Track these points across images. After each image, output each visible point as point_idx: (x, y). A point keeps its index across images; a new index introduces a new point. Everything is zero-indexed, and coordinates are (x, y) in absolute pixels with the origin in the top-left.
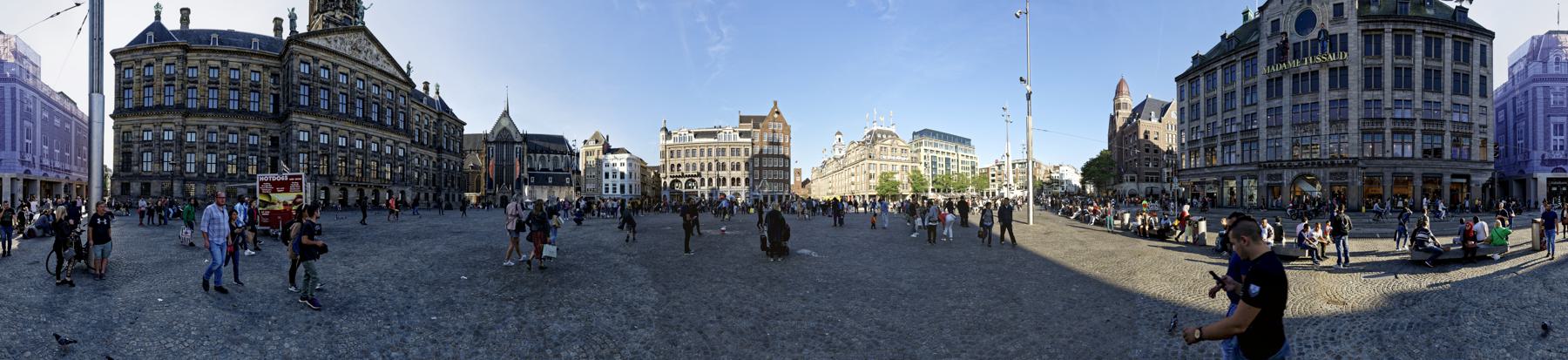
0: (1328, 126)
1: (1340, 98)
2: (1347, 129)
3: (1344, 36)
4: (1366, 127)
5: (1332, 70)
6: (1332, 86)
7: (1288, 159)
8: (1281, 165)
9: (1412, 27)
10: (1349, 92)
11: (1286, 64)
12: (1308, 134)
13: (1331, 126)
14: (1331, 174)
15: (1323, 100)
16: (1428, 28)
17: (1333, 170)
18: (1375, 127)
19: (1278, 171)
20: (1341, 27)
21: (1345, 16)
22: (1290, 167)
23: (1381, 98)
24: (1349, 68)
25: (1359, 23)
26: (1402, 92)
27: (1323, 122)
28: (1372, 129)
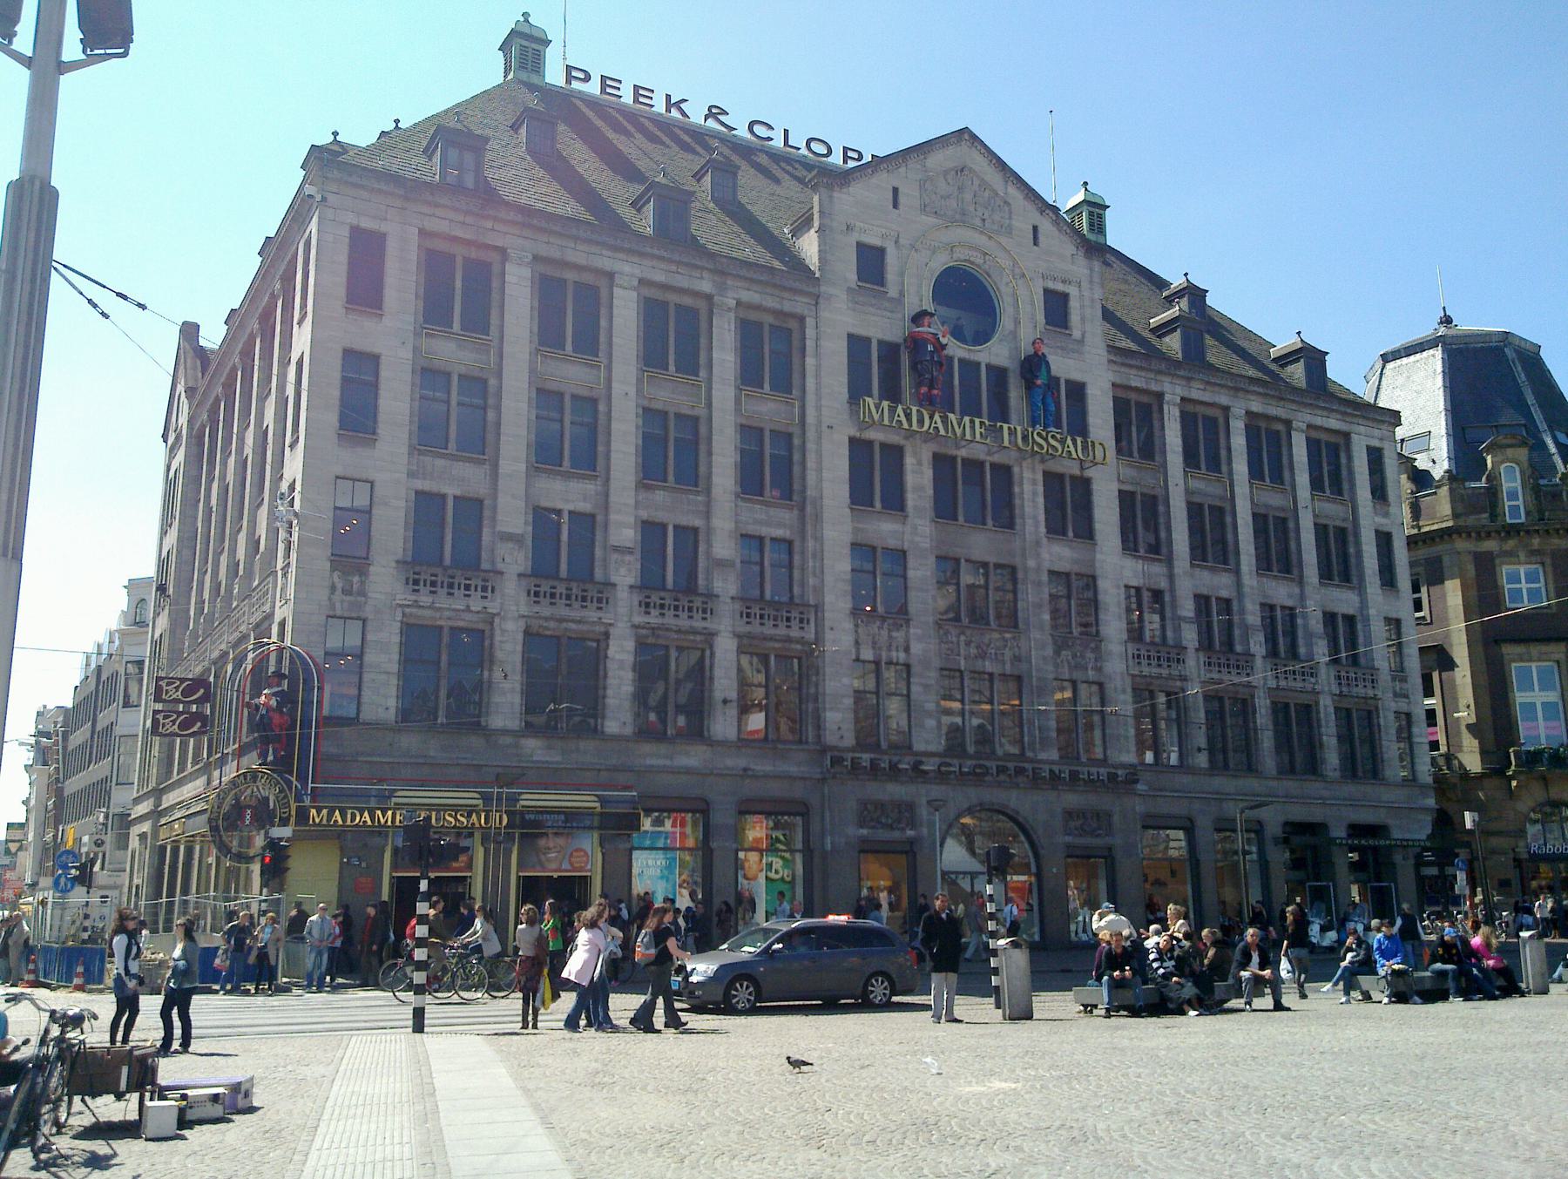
0: (1049, 651)
1: (1076, 569)
2: (1099, 670)
3: (1077, 391)
4: (1146, 671)
5: (1053, 482)
6: (1056, 528)
7: (932, 748)
8: (916, 767)
9: (1223, 399)
10: (1098, 556)
11: (945, 420)
12: (989, 666)
13: (1057, 653)
14: (1069, 814)
15: (1031, 563)
16: (1256, 406)
17: (1072, 799)
18: (1165, 672)
19: (895, 791)
20: (1071, 362)
21: (1077, 334)
22: (942, 776)
23: (1163, 584)
24: (1095, 487)
25: (1110, 361)
26: (1206, 574)
27: (1035, 634)
28: (1159, 677)
